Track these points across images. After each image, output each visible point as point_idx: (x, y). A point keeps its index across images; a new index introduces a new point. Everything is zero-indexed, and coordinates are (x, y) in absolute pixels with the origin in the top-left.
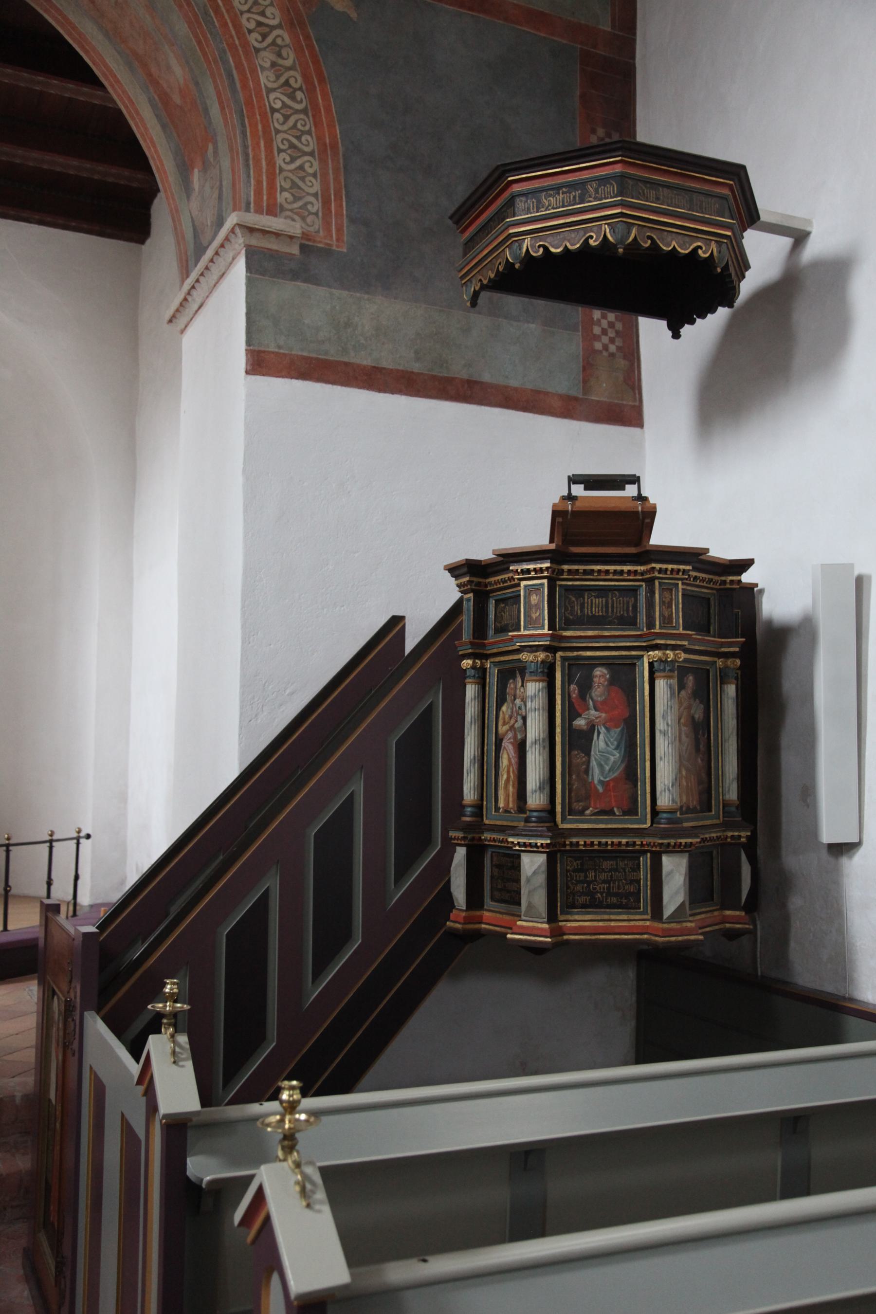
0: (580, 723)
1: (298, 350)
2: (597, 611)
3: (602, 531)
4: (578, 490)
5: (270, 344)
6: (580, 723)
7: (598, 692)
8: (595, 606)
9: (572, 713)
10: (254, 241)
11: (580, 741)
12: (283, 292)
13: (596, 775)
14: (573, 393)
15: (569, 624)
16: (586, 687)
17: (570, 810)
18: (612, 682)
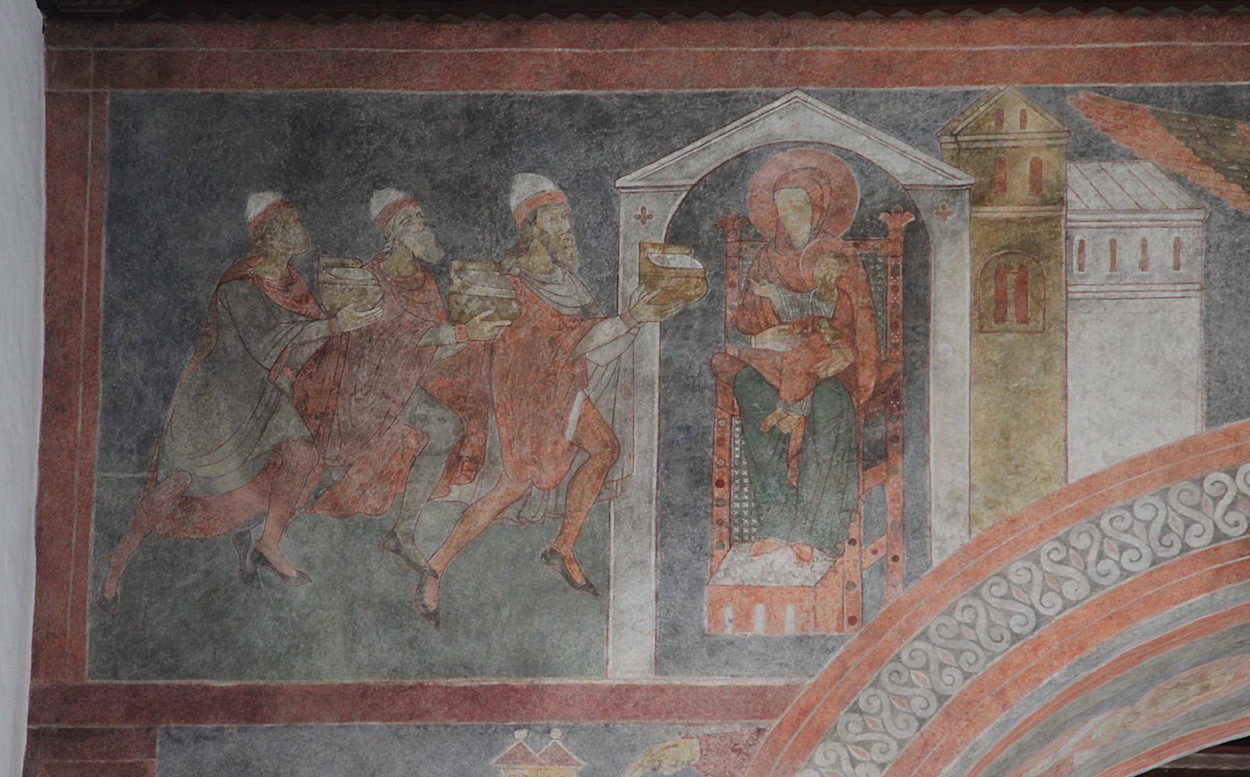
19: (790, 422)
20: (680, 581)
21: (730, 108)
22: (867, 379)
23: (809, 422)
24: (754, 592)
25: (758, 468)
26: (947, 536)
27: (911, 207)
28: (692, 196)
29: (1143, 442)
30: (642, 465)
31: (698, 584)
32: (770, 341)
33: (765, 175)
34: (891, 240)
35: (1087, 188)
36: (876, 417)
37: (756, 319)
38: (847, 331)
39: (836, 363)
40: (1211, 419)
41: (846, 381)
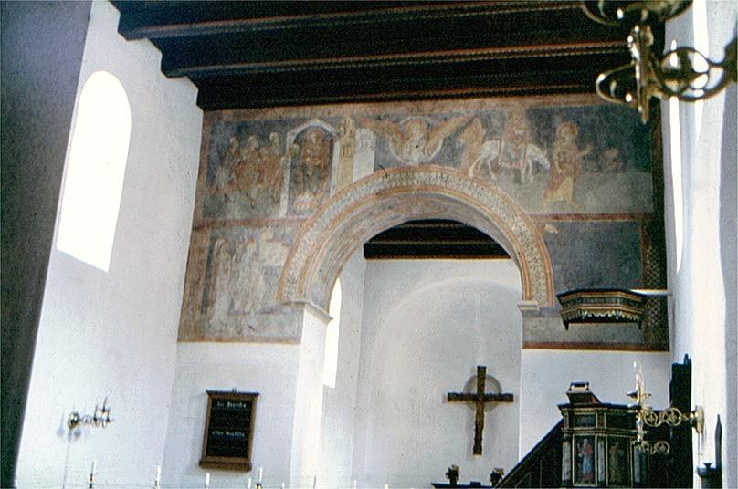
0: (580, 455)
1: (539, 341)
2: (584, 422)
3: (579, 401)
4: (573, 387)
5: (529, 339)
6: (580, 455)
7: (584, 445)
8: (584, 420)
9: (577, 452)
10: (522, 309)
11: (579, 461)
12: (534, 322)
13: (584, 471)
14: (640, 342)
15: (577, 426)
16: (582, 444)
17: (576, 481)
18: (589, 443)
19: (310, 173)
20: (291, 201)
21: (304, 120)
22: (323, 165)
23: (313, 174)
24: (303, 202)
25: (304, 182)
26: (333, 192)
27: (331, 136)
28: (298, 135)
29: (363, 175)
30: (287, 181)
31: (294, 200)
32: (308, 159)
33: (308, 132)
34: (328, 142)
35: (359, 133)
36: (324, 171)
37: (305, 157)
38: (320, 158)
39: (318, 162)
40: (375, 170)
41: (319, 166)
